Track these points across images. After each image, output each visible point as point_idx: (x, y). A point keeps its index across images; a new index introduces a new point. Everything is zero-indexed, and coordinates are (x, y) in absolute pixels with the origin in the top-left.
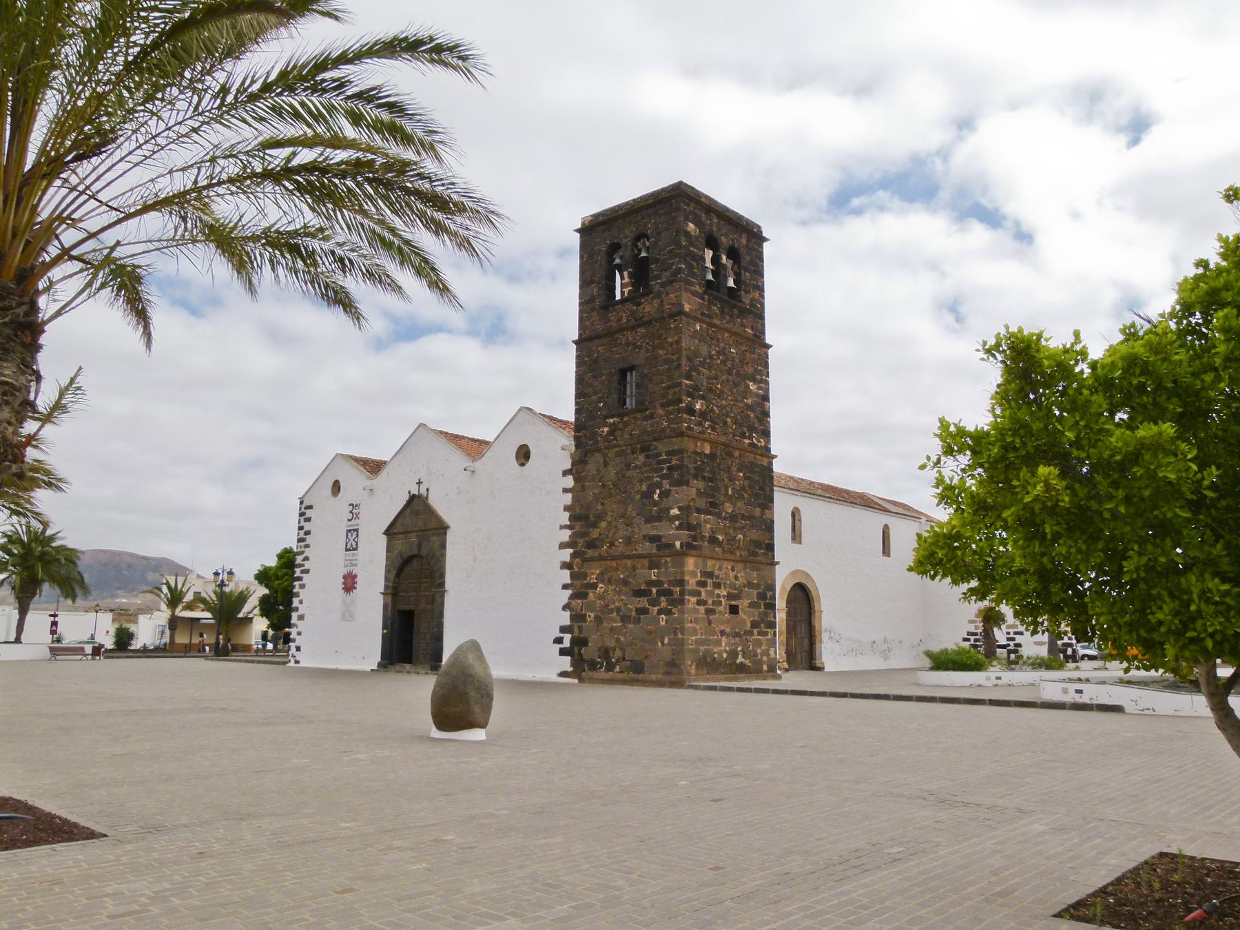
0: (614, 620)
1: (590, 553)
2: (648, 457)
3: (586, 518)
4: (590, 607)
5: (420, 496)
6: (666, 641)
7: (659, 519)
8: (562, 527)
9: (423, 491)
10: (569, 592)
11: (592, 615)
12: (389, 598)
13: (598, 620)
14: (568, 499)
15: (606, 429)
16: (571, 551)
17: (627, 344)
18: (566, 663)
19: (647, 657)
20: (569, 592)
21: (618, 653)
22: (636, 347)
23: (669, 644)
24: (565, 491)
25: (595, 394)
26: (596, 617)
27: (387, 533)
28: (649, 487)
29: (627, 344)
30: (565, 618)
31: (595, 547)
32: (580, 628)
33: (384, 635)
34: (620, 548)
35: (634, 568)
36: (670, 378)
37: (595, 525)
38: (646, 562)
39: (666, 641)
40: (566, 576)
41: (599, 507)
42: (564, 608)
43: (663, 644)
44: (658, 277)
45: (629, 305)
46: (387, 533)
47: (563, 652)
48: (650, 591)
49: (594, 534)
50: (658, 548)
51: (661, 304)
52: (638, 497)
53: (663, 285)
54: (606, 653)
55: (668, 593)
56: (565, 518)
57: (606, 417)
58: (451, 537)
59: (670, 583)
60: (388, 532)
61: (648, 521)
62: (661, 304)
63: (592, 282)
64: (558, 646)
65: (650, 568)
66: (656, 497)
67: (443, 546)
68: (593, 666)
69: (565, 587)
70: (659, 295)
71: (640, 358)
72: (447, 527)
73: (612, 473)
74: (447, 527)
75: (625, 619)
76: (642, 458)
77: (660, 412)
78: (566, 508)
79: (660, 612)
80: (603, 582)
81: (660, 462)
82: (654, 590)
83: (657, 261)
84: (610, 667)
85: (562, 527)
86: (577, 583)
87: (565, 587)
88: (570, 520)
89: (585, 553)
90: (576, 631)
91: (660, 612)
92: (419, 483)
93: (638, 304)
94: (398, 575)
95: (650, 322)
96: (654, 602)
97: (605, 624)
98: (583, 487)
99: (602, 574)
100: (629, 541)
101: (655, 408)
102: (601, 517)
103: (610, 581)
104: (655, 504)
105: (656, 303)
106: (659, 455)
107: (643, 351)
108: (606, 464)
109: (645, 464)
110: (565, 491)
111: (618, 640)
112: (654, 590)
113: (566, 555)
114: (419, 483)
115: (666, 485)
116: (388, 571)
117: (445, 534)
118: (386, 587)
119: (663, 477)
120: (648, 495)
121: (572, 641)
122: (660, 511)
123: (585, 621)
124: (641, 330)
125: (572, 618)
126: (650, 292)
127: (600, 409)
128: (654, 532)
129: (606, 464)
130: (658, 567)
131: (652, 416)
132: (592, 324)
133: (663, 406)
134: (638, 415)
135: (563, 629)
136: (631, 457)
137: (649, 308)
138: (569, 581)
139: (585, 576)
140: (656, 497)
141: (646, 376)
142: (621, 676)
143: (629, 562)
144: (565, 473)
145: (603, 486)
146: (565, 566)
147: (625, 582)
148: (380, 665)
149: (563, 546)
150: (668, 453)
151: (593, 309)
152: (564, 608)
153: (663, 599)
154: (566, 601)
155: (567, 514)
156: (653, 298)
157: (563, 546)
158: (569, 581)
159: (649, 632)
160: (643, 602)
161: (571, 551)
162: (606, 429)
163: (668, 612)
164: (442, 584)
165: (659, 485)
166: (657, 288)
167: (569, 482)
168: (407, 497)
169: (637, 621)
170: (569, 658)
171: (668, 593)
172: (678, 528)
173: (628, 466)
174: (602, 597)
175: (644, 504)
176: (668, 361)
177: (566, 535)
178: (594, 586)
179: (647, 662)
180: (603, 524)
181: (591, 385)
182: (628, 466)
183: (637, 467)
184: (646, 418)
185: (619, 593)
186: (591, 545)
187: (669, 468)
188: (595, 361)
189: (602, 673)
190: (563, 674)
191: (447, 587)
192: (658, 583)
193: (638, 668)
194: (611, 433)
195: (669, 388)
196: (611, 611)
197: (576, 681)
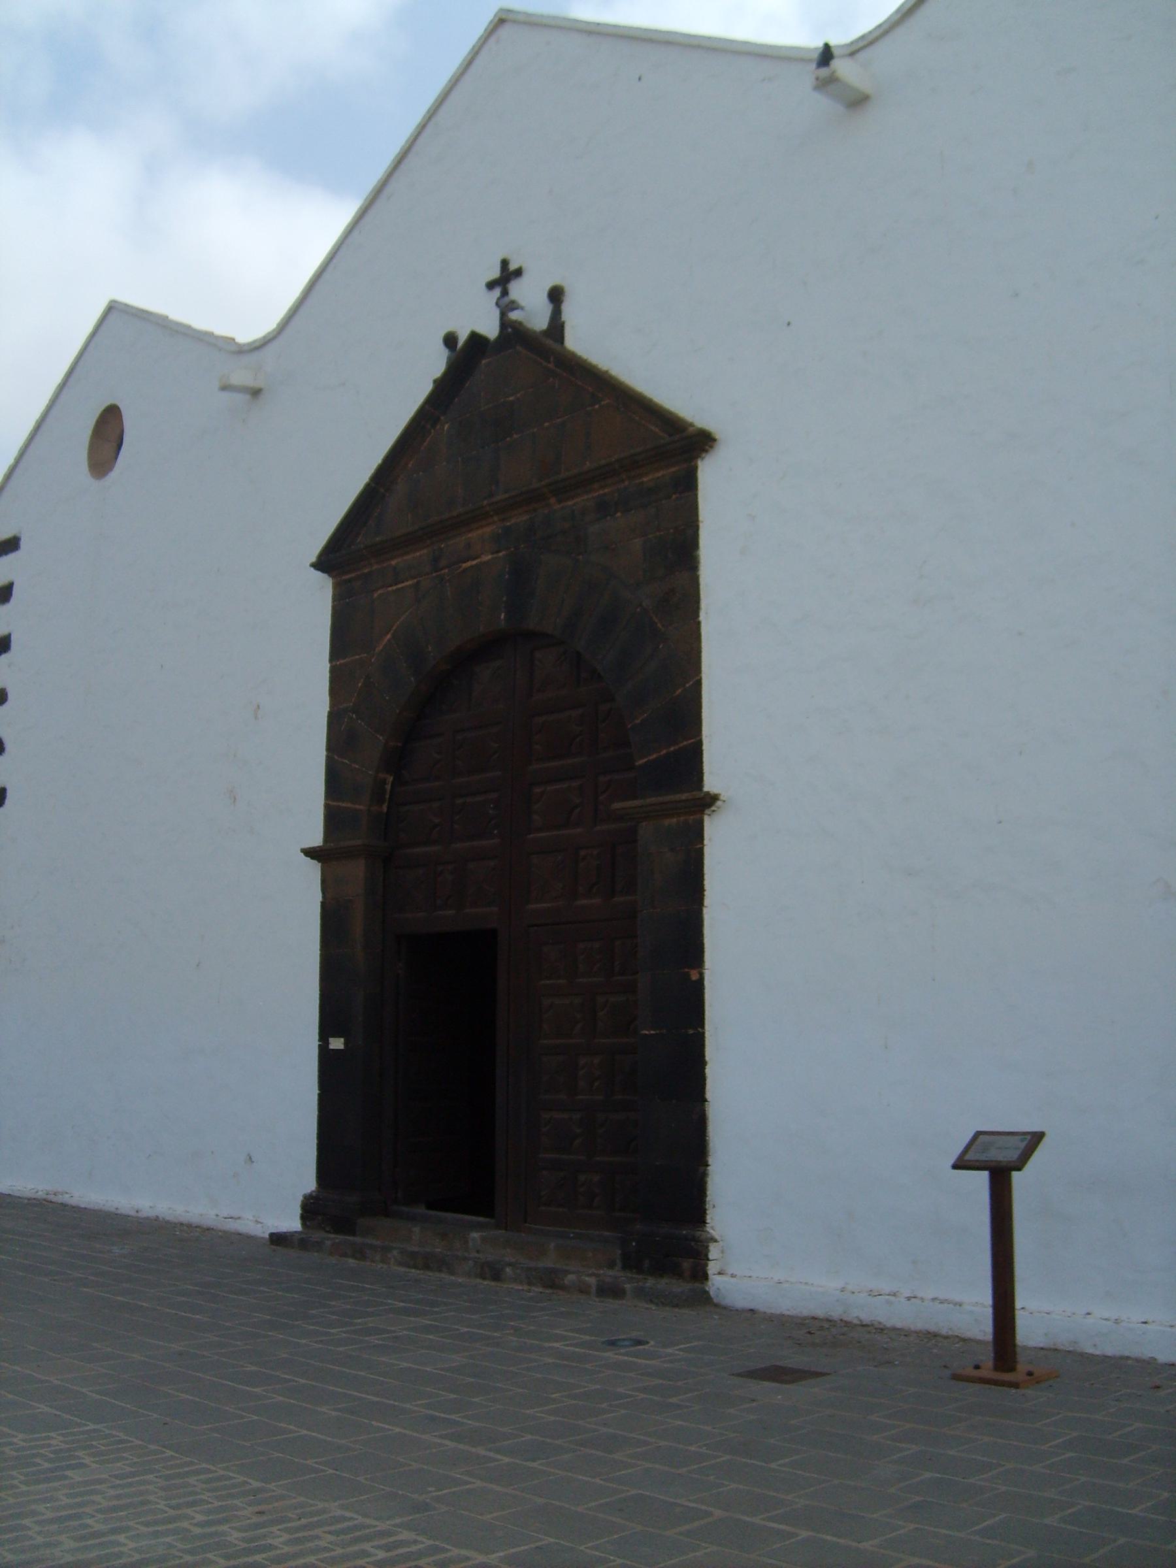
5: (513, 334)
9: (534, 312)
12: (356, 871)
27: (323, 564)
33: (327, 1058)
46: (330, 560)
58: (722, 494)
60: (345, 555)
67: (679, 550)
72: (700, 442)
74: (700, 442)
92: (507, 276)
94: (396, 761)
114: (507, 276)
116: (341, 740)
117: (688, 484)
118: (333, 820)
148: (311, 1209)
164: (690, 762)
168: (436, 363)
191: (711, 783)
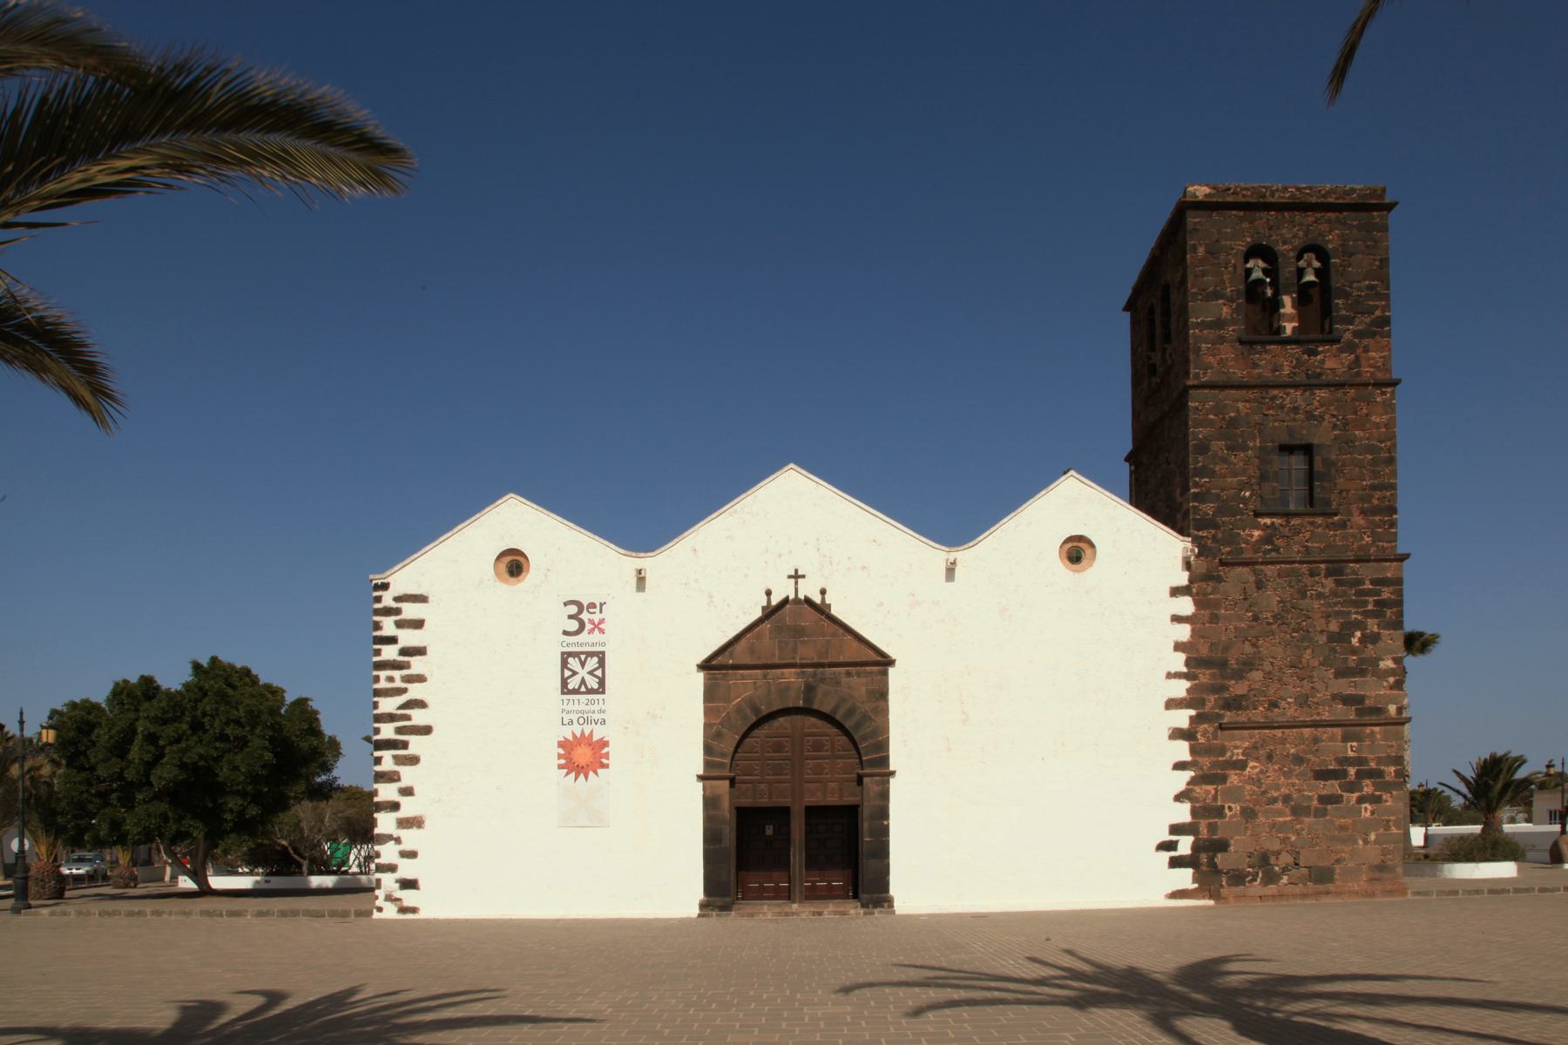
0: (1280, 813)
1: (1228, 717)
2: (1338, 583)
3: (1223, 664)
4: (1235, 794)
6: (1373, 837)
7: (1361, 672)
8: (1170, 676)
10: (1187, 775)
11: (1236, 807)
13: (1248, 814)
14: (1184, 632)
15: (1257, 533)
16: (1193, 712)
17: (1295, 410)
18: (1184, 878)
19: (1338, 861)
20: (1187, 775)
21: (1286, 859)
22: (1310, 416)
23: (1376, 842)
24: (1177, 619)
25: (1235, 475)
26: (1244, 811)
28: (1342, 626)
29: (1295, 410)
30: (1183, 813)
31: (1239, 707)
32: (1212, 828)
34: (1289, 711)
35: (1316, 740)
36: (1375, 474)
37: (1239, 675)
38: (1338, 731)
39: (1373, 837)
40: (1182, 750)
41: (1248, 648)
42: (1179, 798)
43: (1366, 842)
44: (1350, 321)
45: (1294, 350)
47: (1175, 863)
48: (1345, 774)
49: (1239, 688)
50: (1359, 712)
51: (1357, 361)
52: (1323, 639)
53: (1356, 334)
54: (1264, 860)
55: (1376, 774)
56: (1178, 662)
57: (1257, 514)
59: (1379, 761)
61: (1338, 675)
62: (1357, 361)
63: (1216, 295)
64: (1166, 856)
65: (1345, 739)
66: (1355, 641)
68: (1238, 878)
69: (1180, 766)
70: (1350, 348)
71: (1322, 435)
73: (1271, 600)
75: (1298, 811)
76: (1329, 583)
77: (1358, 520)
78: (1178, 647)
79: (1361, 800)
80: (1257, 759)
81: (1361, 593)
82: (1352, 771)
83: (1347, 296)
84: (1271, 878)
85: (1170, 676)
86: (1206, 761)
87: (1180, 766)
88: (1187, 664)
89: (1220, 716)
90: (1204, 833)
91: (1361, 800)
93: (1314, 353)
95: (1340, 385)
96: (1351, 788)
97: (1261, 819)
98: (1214, 618)
99: (1255, 747)
100: (1303, 701)
101: (1350, 514)
102: (1249, 665)
103: (1270, 757)
104: (1354, 651)
105: (1348, 358)
106: (1360, 582)
107: (1325, 423)
108: (1260, 585)
109: (1334, 594)
110: (1177, 619)
111: (1284, 841)
112: (1352, 771)
113: (1183, 718)
115: (1373, 625)
119: (1367, 614)
120: (1342, 637)
121: (1195, 847)
122: (1362, 661)
123: (1220, 812)
124: (1322, 394)
125: (1194, 812)
126: (1338, 341)
127: (1245, 500)
128: (1351, 691)
129: (1260, 585)
130: (1358, 738)
131: (1343, 525)
132: (1221, 361)
133: (1363, 512)
134: (1319, 520)
135: (1176, 829)
136: (1308, 581)
137: (1331, 362)
138: (1187, 757)
139: (1223, 751)
140: (1355, 641)
141: (1333, 464)
142: (1291, 889)
143: (1307, 732)
144: (1176, 592)
145: (1256, 618)
146: (1177, 734)
147: (1299, 760)
149: (1172, 704)
150: (1373, 582)
151: (1222, 340)
152: (1179, 798)
153: (1368, 782)
154: (1181, 787)
155: (1182, 657)
156: (1341, 350)
157: (1172, 704)
158: (1187, 757)
159: (1342, 828)
160: (1332, 787)
161: (1193, 712)
162: (1257, 533)
163: (1376, 800)
165: (1360, 625)
166: (1347, 336)
167: (1186, 606)
169: (1320, 813)
170: (1189, 872)
171: (1376, 774)
172: (1391, 688)
173: (1303, 595)
174: (1255, 781)
175: (1333, 650)
176: (1371, 449)
177: (1180, 688)
178: (1242, 765)
179: (1337, 868)
180: (1257, 675)
181: (1224, 460)
182: (1303, 595)
183: (1320, 596)
184: (1334, 526)
185: (1288, 775)
186: (1234, 704)
187: (1377, 603)
188: (1233, 423)
189: (1256, 888)
190: (1175, 895)
192: (1360, 761)
193: (1322, 876)
194: (1266, 540)
195: (1374, 488)
196: (1275, 800)
197: (1211, 902)
